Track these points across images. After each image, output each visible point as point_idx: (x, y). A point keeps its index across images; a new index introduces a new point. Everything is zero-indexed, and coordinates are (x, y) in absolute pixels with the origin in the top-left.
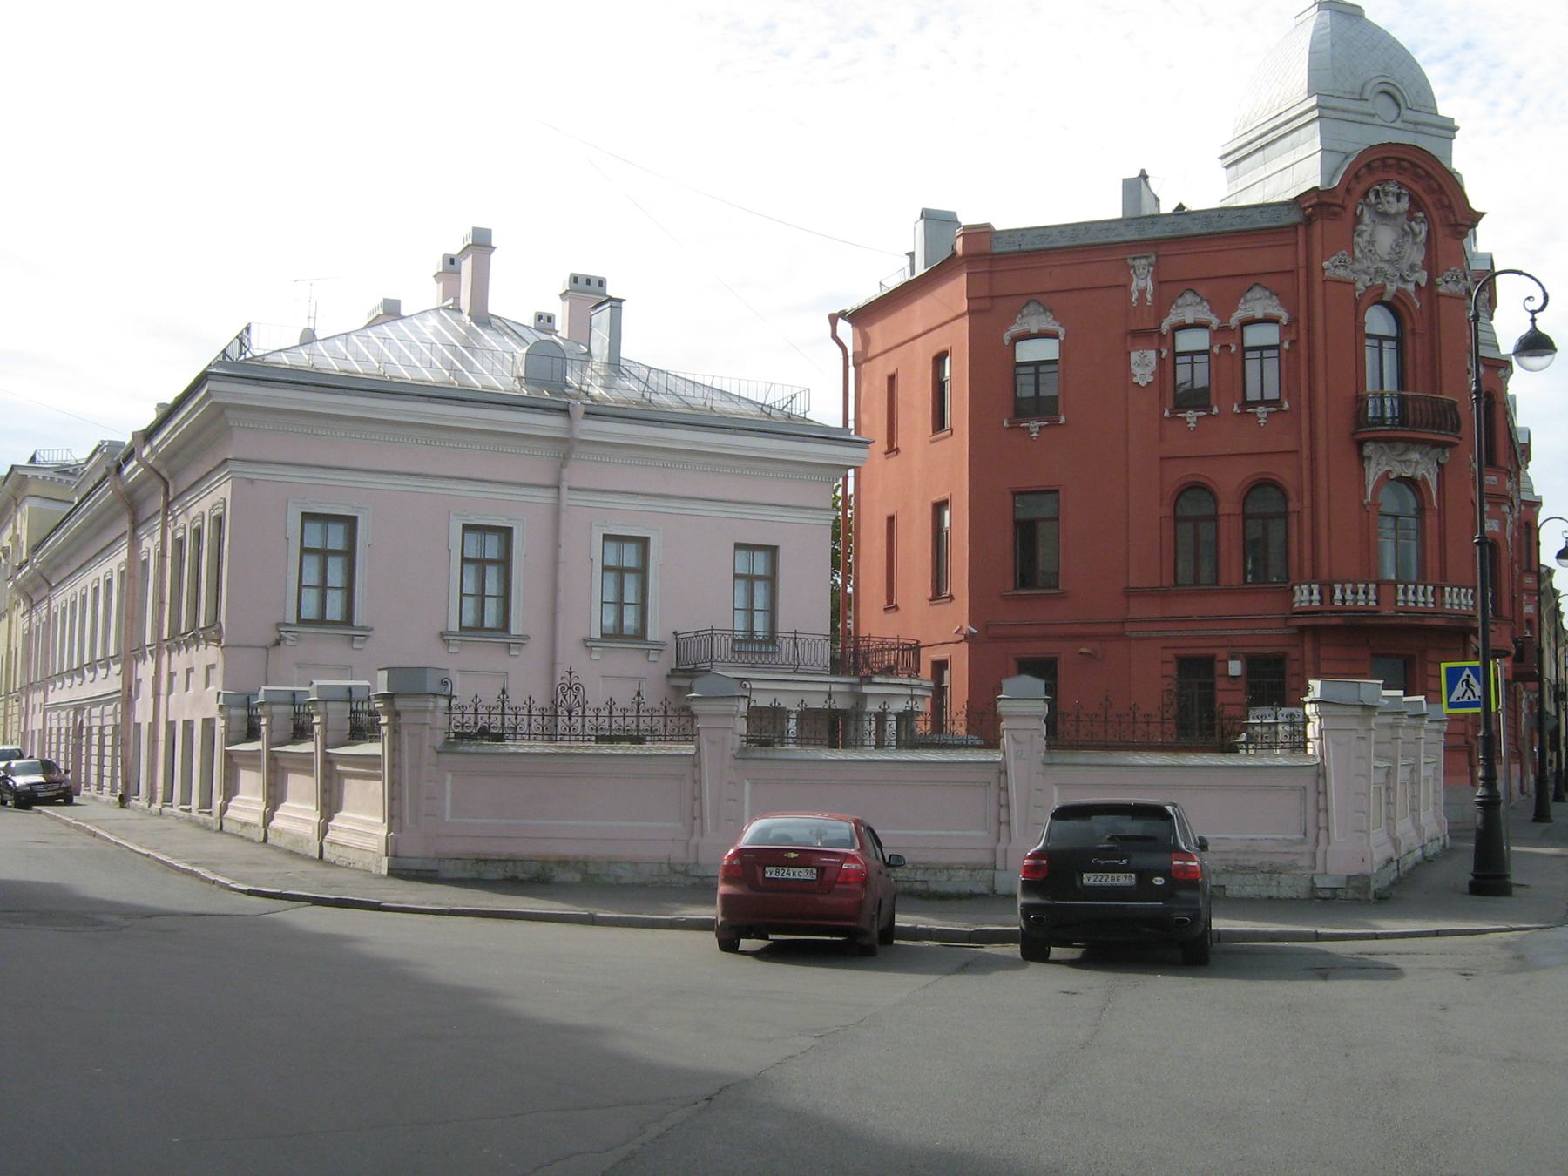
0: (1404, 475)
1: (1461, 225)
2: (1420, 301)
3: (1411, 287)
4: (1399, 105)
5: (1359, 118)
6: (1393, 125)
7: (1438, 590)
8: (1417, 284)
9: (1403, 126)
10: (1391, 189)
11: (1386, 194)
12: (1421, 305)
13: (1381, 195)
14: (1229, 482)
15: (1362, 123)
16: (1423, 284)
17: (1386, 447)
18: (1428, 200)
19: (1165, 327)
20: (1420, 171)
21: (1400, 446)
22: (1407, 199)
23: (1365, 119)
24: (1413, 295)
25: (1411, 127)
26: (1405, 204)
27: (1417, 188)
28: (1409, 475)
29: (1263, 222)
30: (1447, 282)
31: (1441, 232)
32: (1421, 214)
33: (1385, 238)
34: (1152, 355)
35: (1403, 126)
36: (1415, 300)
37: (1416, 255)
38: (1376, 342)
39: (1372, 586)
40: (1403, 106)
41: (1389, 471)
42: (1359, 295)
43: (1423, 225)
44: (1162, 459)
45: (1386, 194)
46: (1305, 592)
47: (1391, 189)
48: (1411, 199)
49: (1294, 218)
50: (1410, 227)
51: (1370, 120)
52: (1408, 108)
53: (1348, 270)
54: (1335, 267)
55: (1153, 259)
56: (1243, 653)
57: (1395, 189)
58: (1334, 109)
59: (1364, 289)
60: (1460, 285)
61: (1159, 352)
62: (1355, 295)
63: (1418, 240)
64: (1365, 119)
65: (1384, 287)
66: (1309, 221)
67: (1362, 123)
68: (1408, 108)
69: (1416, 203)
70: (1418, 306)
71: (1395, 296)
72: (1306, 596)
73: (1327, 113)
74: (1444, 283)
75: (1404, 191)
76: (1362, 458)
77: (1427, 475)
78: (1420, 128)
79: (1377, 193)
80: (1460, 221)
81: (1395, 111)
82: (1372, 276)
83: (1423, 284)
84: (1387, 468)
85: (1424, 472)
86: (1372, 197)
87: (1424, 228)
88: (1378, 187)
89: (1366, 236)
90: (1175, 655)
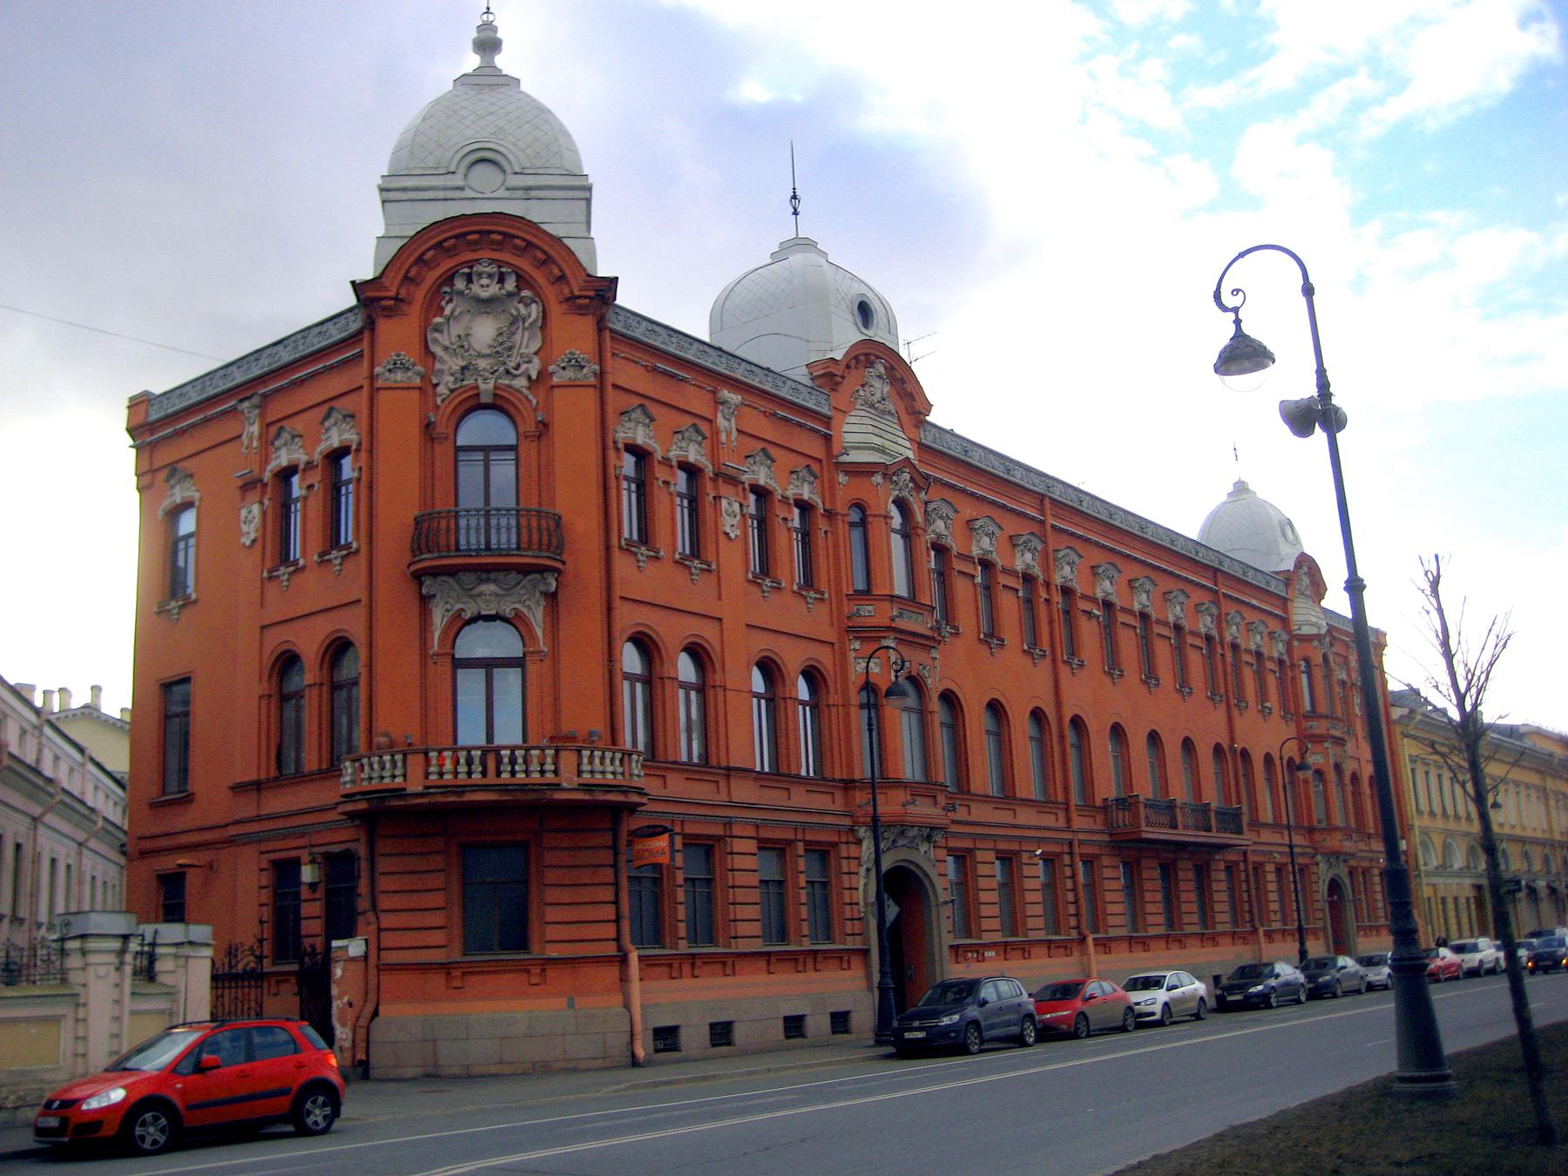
0: (483, 613)
1: (579, 297)
2: (535, 396)
3: (521, 383)
4: (504, 172)
5: (441, 194)
6: (493, 195)
7: (626, 757)
8: (529, 378)
9: (507, 194)
10: (486, 269)
11: (480, 275)
12: (537, 403)
13: (474, 279)
14: (309, 643)
15: (445, 200)
16: (534, 377)
17: (451, 580)
18: (538, 276)
19: (267, 476)
20: (518, 242)
21: (466, 578)
22: (513, 278)
23: (450, 194)
24: (524, 390)
25: (519, 194)
26: (510, 285)
27: (523, 263)
28: (494, 612)
29: (336, 334)
30: (564, 368)
31: (556, 310)
32: (525, 293)
33: (484, 331)
34: (256, 509)
35: (507, 194)
36: (531, 397)
37: (526, 343)
38: (480, 456)
39: (399, 757)
40: (509, 171)
41: (462, 610)
42: (443, 401)
43: (534, 306)
44: (263, 628)
45: (480, 275)
46: (376, 766)
47: (486, 269)
48: (519, 277)
49: (355, 324)
50: (518, 310)
51: (458, 194)
52: (516, 173)
53: (410, 373)
54: (390, 370)
55: (256, 400)
56: (321, 854)
57: (492, 269)
58: (404, 189)
59: (448, 392)
60: (585, 371)
61: (261, 503)
62: (436, 401)
63: (526, 325)
64: (450, 194)
65: (477, 387)
66: (370, 325)
67: (445, 200)
68: (516, 173)
69: (523, 281)
70: (534, 402)
71: (495, 395)
72: (382, 773)
73: (392, 195)
74: (561, 371)
75: (504, 270)
76: (425, 601)
77: (525, 610)
78: (533, 194)
79: (469, 278)
80: (577, 293)
81: (499, 177)
82: (459, 375)
83: (534, 377)
84: (459, 606)
85: (518, 606)
86: (460, 284)
87: (535, 310)
88: (466, 270)
89: (456, 329)
90: (270, 861)
